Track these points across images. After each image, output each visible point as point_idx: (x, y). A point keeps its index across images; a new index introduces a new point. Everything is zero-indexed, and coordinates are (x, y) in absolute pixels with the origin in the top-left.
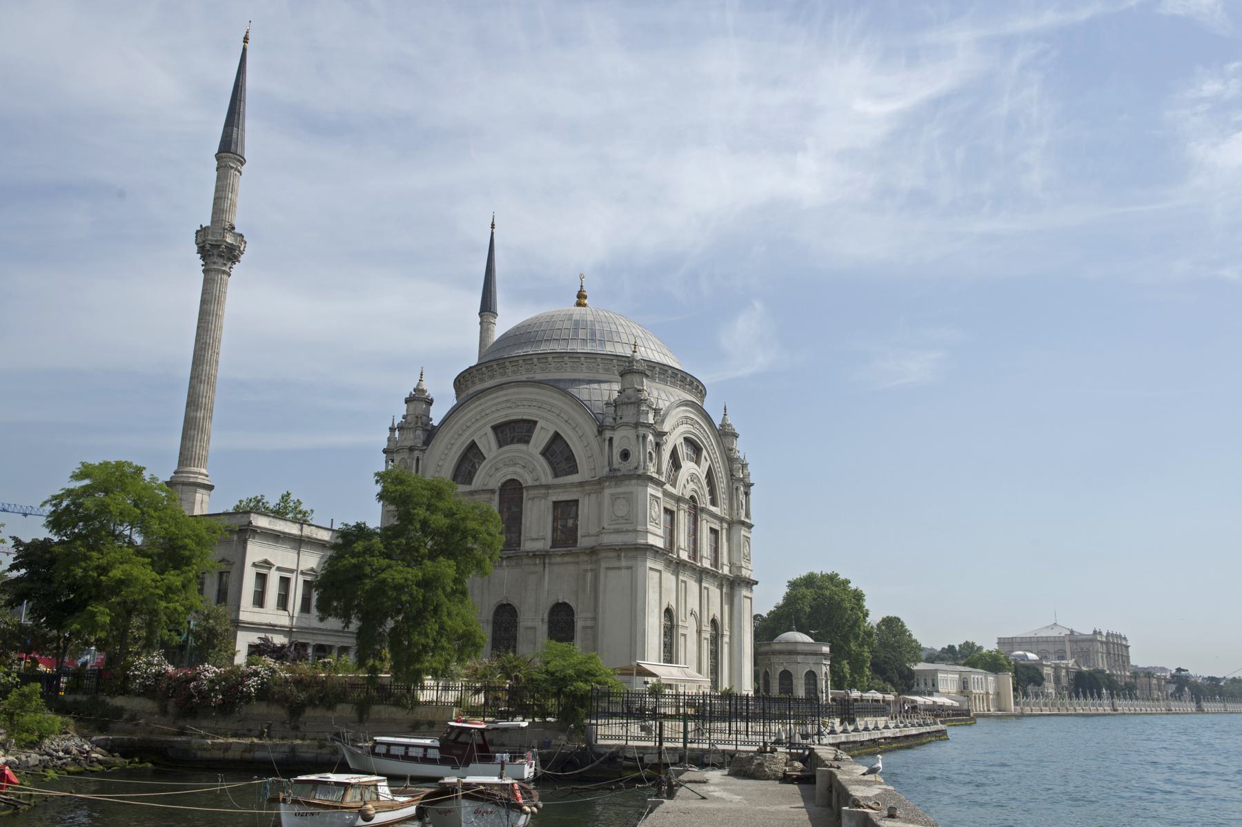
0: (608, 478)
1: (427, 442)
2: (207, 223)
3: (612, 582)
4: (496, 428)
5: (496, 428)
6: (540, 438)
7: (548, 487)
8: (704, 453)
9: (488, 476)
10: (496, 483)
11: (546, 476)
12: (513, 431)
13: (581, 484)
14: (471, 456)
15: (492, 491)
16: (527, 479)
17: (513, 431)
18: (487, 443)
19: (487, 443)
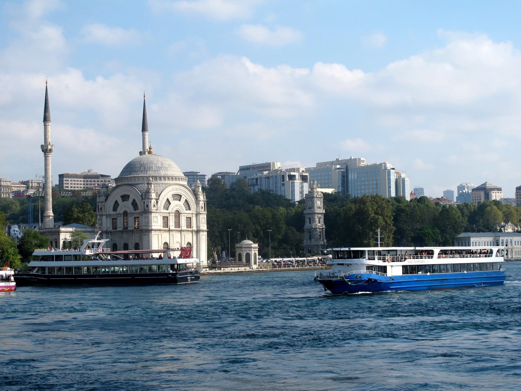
0: (143, 212)
1: (106, 200)
2: (43, 144)
3: (145, 238)
4: (122, 197)
5: (122, 197)
6: (131, 200)
7: (133, 213)
8: (183, 196)
9: (120, 210)
10: (122, 212)
11: (133, 211)
12: (125, 198)
13: (139, 213)
14: (116, 205)
15: (121, 214)
16: (129, 211)
17: (125, 198)
18: (120, 201)
19: (120, 201)
